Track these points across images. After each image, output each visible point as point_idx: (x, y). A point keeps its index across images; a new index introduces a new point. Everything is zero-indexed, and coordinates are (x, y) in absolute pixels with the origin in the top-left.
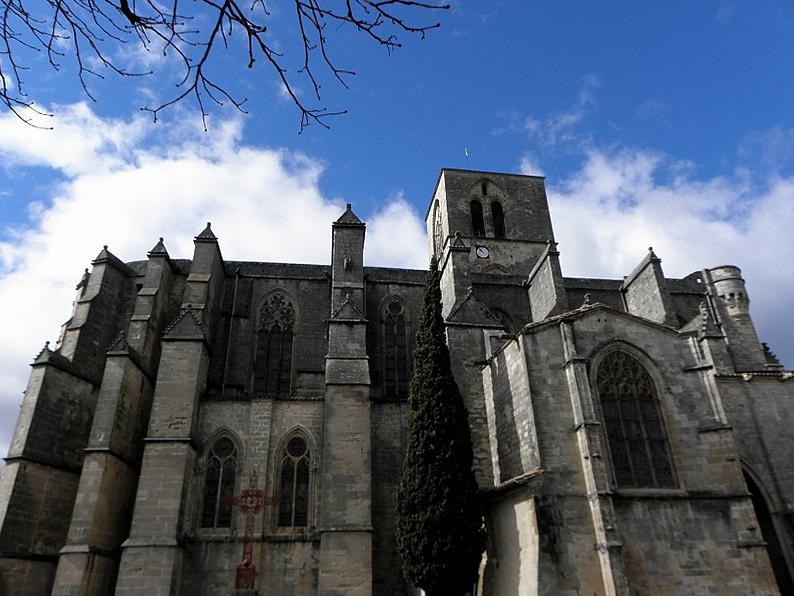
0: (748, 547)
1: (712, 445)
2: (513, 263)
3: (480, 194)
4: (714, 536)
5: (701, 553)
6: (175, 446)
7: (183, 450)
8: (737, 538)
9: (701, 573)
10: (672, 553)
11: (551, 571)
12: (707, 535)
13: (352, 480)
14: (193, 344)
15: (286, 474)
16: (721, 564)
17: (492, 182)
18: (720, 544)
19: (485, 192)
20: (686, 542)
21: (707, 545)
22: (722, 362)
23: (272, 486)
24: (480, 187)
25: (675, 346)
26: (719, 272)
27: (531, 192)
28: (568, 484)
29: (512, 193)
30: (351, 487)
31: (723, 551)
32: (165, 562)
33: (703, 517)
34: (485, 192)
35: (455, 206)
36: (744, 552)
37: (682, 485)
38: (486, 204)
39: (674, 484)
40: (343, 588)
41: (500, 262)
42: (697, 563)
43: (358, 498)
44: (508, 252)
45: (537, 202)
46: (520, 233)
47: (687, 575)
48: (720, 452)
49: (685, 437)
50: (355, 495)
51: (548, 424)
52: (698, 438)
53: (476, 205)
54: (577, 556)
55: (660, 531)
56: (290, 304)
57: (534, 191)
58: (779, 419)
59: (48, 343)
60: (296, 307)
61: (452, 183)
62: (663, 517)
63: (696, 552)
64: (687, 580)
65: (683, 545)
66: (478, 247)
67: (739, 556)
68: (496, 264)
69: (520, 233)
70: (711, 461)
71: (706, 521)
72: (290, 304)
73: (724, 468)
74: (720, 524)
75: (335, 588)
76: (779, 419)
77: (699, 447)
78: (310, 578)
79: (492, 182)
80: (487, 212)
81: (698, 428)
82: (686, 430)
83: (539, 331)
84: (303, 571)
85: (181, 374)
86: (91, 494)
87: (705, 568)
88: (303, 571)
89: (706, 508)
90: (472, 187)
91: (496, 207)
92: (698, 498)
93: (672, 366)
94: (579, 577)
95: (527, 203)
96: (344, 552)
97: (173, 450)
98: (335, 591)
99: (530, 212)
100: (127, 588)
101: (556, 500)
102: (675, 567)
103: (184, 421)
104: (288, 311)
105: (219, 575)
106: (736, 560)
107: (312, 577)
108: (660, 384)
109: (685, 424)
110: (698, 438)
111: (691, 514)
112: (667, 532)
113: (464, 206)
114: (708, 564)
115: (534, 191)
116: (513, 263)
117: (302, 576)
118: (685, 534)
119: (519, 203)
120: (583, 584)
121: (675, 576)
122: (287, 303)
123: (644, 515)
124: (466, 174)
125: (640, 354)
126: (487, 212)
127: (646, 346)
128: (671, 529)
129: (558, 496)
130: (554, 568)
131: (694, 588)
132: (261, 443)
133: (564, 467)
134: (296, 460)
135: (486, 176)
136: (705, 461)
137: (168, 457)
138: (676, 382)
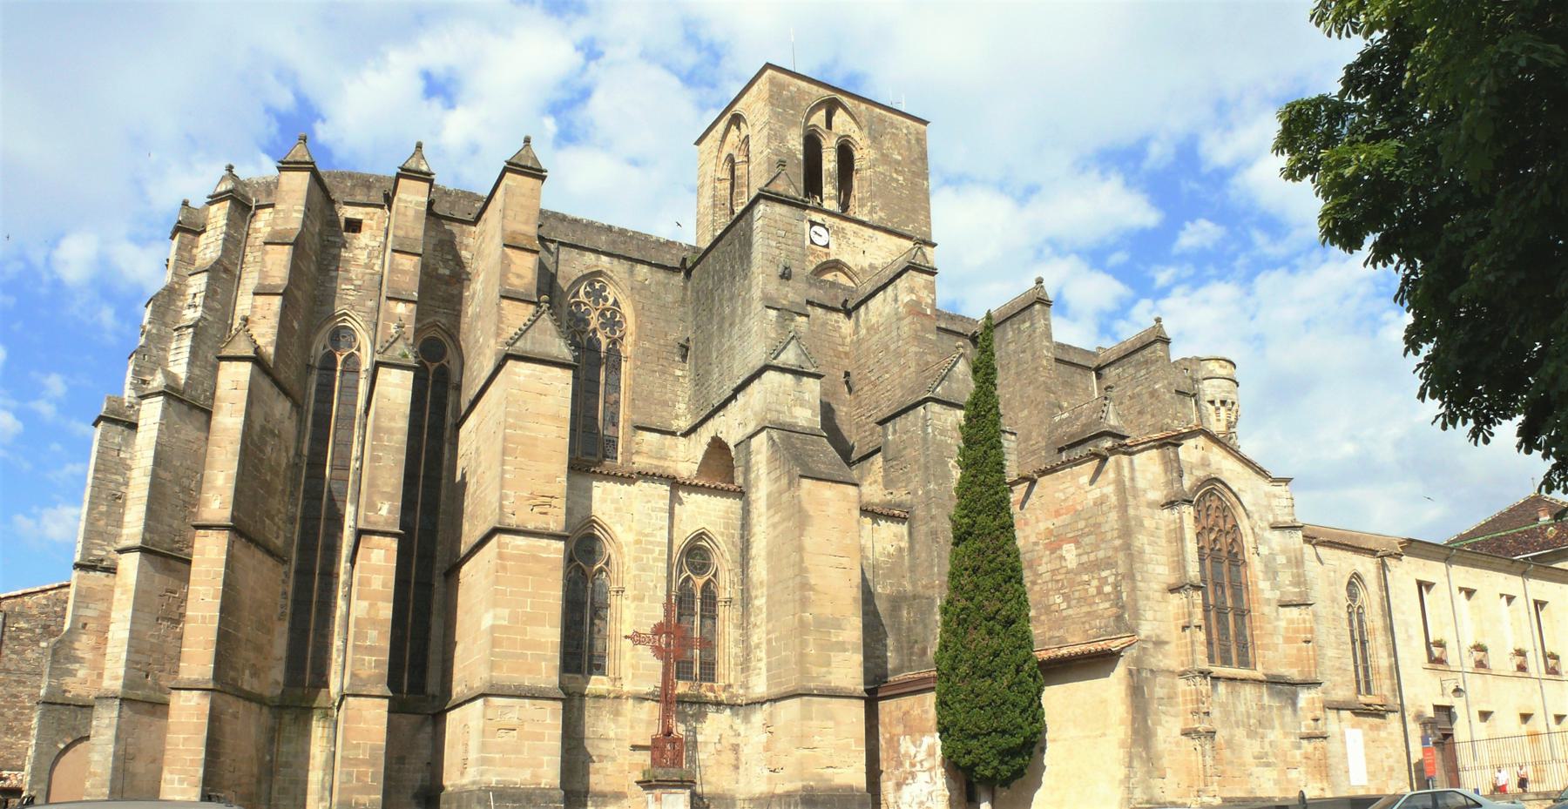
0: (1309, 738)
1: (1291, 621)
2: (866, 265)
3: (823, 125)
4: (1283, 726)
5: (1271, 743)
6: (544, 542)
7: (556, 550)
8: (1300, 728)
9: (1268, 765)
10: (1247, 742)
11: (1141, 757)
12: (1277, 723)
13: (837, 624)
14: (557, 371)
15: (681, 602)
16: (1285, 755)
17: (845, 109)
18: (1286, 734)
19: (829, 125)
20: (1260, 730)
21: (1274, 735)
23: (340, 594)
24: (823, 113)
25: (1266, 494)
26: (1213, 366)
27: (904, 142)
28: (1160, 657)
29: (875, 138)
30: (837, 636)
31: (1287, 743)
32: (548, 721)
33: (1276, 703)
35: (783, 140)
36: (1305, 742)
37: (1259, 667)
39: (1244, 663)
40: (831, 770)
41: (845, 258)
42: (1266, 754)
43: (845, 650)
44: (858, 242)
45: (913, 162)
46: (883, 215)
47: (1257, 766)
48: (1297, 631)
49: (1266, 610)
50: (842, 647)
51: (1143, 580)
52: (1277, 611)
53: (812, 144)
54: (1165, 742)
55: (1240, 718)
56: (616, 303)
57: (909, 142)
60: (627, 309)
61: (780, 94)
62: (1243, 702)
63: (1267, 741)
64: (1257, 771)
65: (1256, 733)
67: (1299, 748)
69: (883, 215)
70: (1288, 640)
71: (1277, 707)
72: (616, 303)
73: (1299, 650)
74: (1289, 711)
75: (822, 771)
77: (1277, 623)
78: (728, 757)
79: (845, 109)
80: (829, 163)
81: (1279, 601)
82: (1268, 602)
83: (1139, 452)
84: (718, 746)
85: (542, 420)
86: (380, 604)
87: (1272, 759)
88: (718, 746)
89: (1279, 693)
91: (845, 153)
92: (1276, 683)
93: (1261, 520)
94: (1165, 765)
95: (898, 163)
96: (831, 724)
97: (546, 549)
98: (821, 775)
99: (901, 178)
100: (497, 756)
101: (1149, 675)
102: (1248, 757)
103: (554, 502)
104: (614, 313)
105: (603, 744)
106: (1298, 753)
107: (732, 756)
108: (1248, 541)
109: (1268, 594)
110: (1277, 611)
111: (1266, 700)
112: (1245, 720)
113: (796, 143)
114: (1276, 756)
115: (909, 142)
116: (866, 265)
117: (719, 752)
118: (1260, 722)
119: (885, 158)
120: (1169, 773)
121: (1247, 767)
122: (611, 301)
123: (1227, 699)
124: (804, 84)
125: (1234, 499)
126: (829, 163)
127: (1240, 490)
128: (1249, 716)
129: (1152, 671)
130: (1144, 755)
131: (1262, 779)
132: (657, 549)
133: (1158, 636)
134: (700, 581)
135: (838, 96)
136: (1281, 640)
137: (536, 559)
138: (1267, 542)
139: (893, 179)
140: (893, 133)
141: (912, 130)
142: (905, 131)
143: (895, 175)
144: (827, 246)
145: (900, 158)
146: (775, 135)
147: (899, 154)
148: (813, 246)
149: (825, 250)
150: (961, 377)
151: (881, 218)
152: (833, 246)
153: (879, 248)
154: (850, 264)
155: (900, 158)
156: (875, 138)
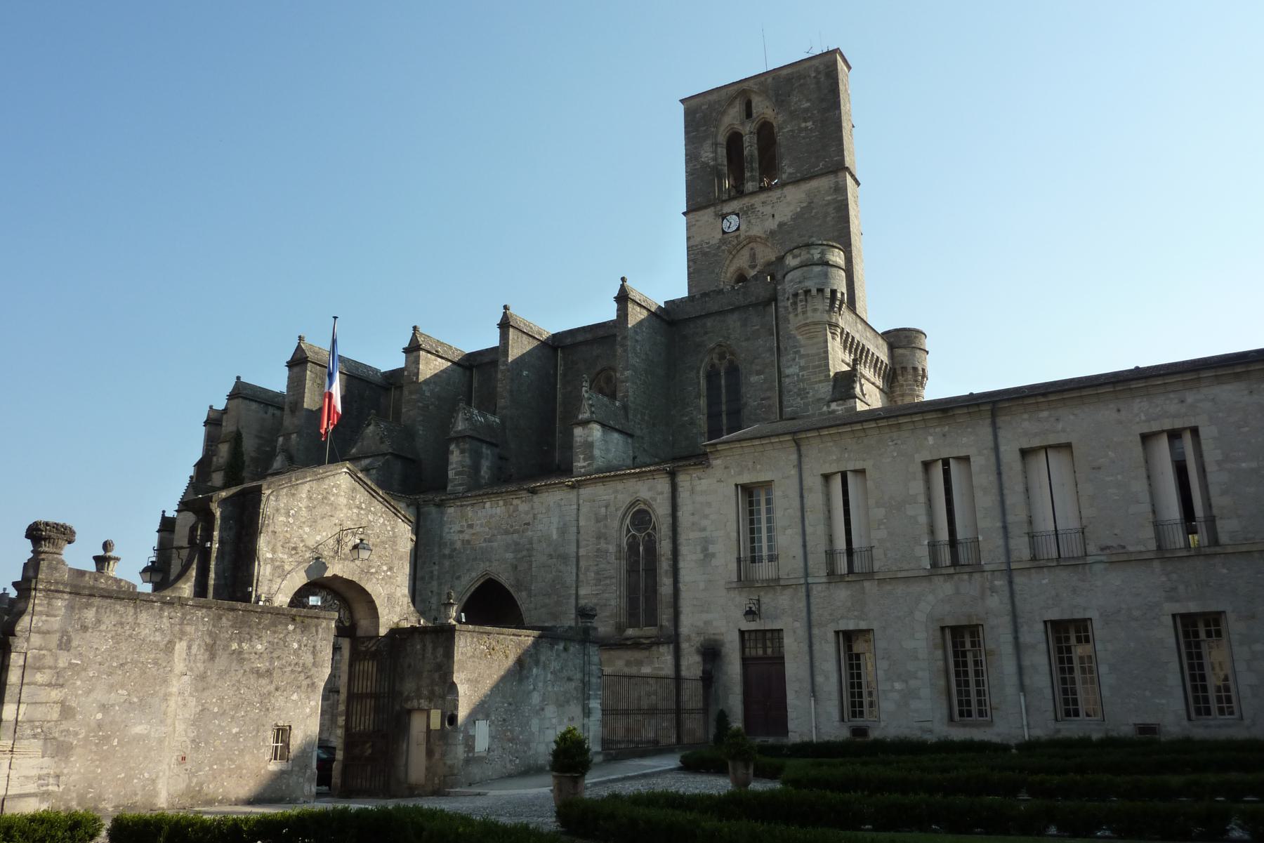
19: (749, 114)
22: (582, 457)
34: (749, 114)
38: (748, 130)
44: (768, 210)
53: (734, 141)
57: (818, 82)
58: (555, 537)
59: (164, 512)
66: (724, 217)
68: (749, 237)
69: (791, 170)
76: (555, 537)
80: (750, 146)
90: (723, 113)
91: (766, 132)
95: (807, 110)
99: (809, 124)
113: (713, 154)
115: (818, 82)
126: (750, 146)
139: (801, 130)
140: (801, 85)
141: (822, 67)
142: (813, 75)
143: (803, 125)
144: (738, 229)
145: (809, 104)
146: (691, 158)
147: (808, 100)
148: (726, 236)
149: (737, 233)
150: (371, 435)
151: (790, 174)
152: (743, 227)
153: (789, 204)
154: (759, 235)
155: (809, 104)
156: (783, 101)
